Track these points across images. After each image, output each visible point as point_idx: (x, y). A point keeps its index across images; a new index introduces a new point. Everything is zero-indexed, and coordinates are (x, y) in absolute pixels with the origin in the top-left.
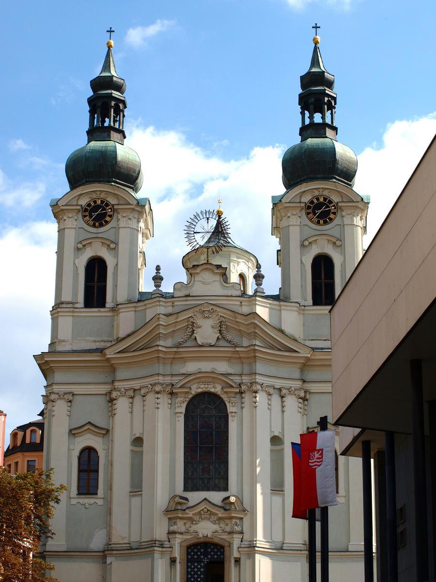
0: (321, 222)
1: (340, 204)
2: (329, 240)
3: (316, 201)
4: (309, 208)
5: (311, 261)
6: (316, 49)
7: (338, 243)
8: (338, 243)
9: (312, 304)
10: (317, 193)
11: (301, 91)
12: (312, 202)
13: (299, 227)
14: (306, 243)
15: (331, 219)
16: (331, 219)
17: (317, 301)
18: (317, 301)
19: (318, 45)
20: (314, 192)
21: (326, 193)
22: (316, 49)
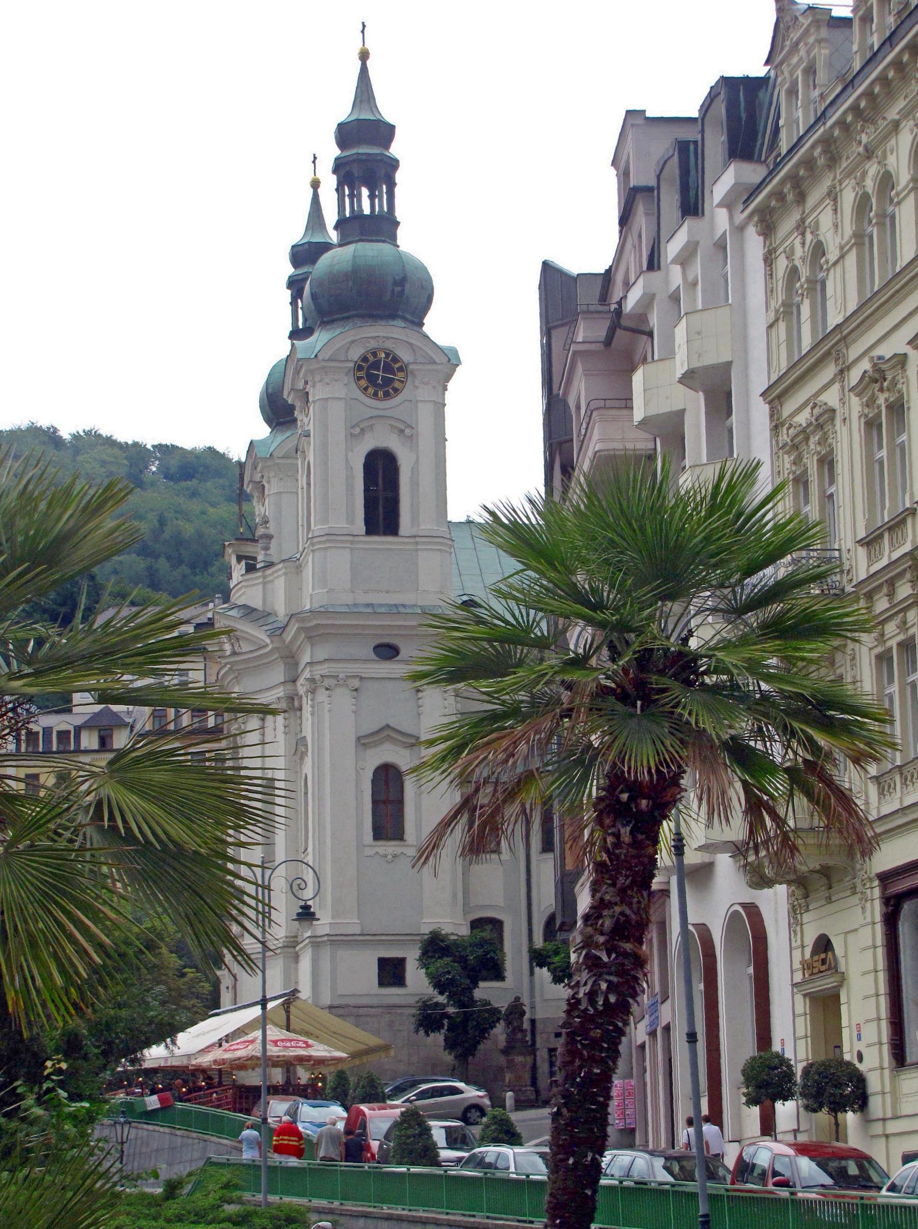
0: (381, 394)
1: (411, 367)
2: (391, 426)
3: (371, 359)
4: (360, 368)
5: (363, 460)
6: (364, 71)
7: (407, 431)
8: (407, 431)
9: (364, 533)
10: (373, 345)
11: (337, 152)
12: (365, 359)
13: (343, 401)
14: (357, 430)
15: (396, 390)
16: (396, 390)
17: (372, 528)
18: (372, 528)
19: (368, 63)
20: (369, 343)
21: (389, 345)
22: (364, 71)
